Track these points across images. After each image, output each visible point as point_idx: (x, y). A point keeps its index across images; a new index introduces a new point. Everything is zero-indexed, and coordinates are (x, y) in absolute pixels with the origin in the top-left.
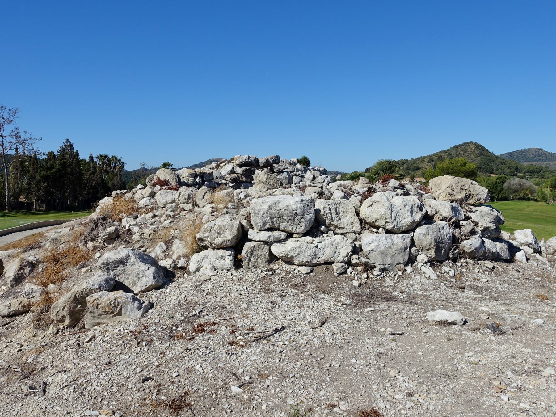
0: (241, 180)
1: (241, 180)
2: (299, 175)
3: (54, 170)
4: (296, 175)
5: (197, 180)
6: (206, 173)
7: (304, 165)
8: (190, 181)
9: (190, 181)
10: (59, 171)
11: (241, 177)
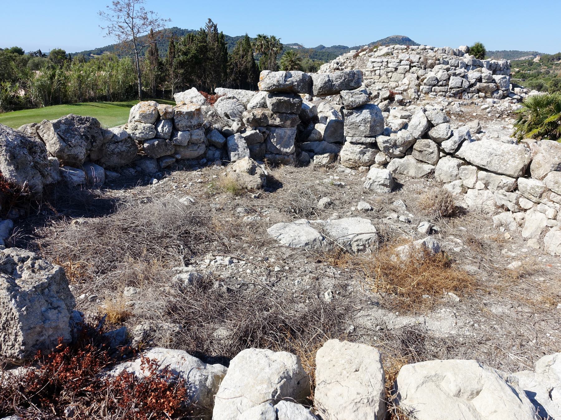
1: (270, 122)
2: (459, 74)
3: (190, 56)
4: (455, 75)
8: (137, 132)
9: (137, 132)
10: (195, 56)
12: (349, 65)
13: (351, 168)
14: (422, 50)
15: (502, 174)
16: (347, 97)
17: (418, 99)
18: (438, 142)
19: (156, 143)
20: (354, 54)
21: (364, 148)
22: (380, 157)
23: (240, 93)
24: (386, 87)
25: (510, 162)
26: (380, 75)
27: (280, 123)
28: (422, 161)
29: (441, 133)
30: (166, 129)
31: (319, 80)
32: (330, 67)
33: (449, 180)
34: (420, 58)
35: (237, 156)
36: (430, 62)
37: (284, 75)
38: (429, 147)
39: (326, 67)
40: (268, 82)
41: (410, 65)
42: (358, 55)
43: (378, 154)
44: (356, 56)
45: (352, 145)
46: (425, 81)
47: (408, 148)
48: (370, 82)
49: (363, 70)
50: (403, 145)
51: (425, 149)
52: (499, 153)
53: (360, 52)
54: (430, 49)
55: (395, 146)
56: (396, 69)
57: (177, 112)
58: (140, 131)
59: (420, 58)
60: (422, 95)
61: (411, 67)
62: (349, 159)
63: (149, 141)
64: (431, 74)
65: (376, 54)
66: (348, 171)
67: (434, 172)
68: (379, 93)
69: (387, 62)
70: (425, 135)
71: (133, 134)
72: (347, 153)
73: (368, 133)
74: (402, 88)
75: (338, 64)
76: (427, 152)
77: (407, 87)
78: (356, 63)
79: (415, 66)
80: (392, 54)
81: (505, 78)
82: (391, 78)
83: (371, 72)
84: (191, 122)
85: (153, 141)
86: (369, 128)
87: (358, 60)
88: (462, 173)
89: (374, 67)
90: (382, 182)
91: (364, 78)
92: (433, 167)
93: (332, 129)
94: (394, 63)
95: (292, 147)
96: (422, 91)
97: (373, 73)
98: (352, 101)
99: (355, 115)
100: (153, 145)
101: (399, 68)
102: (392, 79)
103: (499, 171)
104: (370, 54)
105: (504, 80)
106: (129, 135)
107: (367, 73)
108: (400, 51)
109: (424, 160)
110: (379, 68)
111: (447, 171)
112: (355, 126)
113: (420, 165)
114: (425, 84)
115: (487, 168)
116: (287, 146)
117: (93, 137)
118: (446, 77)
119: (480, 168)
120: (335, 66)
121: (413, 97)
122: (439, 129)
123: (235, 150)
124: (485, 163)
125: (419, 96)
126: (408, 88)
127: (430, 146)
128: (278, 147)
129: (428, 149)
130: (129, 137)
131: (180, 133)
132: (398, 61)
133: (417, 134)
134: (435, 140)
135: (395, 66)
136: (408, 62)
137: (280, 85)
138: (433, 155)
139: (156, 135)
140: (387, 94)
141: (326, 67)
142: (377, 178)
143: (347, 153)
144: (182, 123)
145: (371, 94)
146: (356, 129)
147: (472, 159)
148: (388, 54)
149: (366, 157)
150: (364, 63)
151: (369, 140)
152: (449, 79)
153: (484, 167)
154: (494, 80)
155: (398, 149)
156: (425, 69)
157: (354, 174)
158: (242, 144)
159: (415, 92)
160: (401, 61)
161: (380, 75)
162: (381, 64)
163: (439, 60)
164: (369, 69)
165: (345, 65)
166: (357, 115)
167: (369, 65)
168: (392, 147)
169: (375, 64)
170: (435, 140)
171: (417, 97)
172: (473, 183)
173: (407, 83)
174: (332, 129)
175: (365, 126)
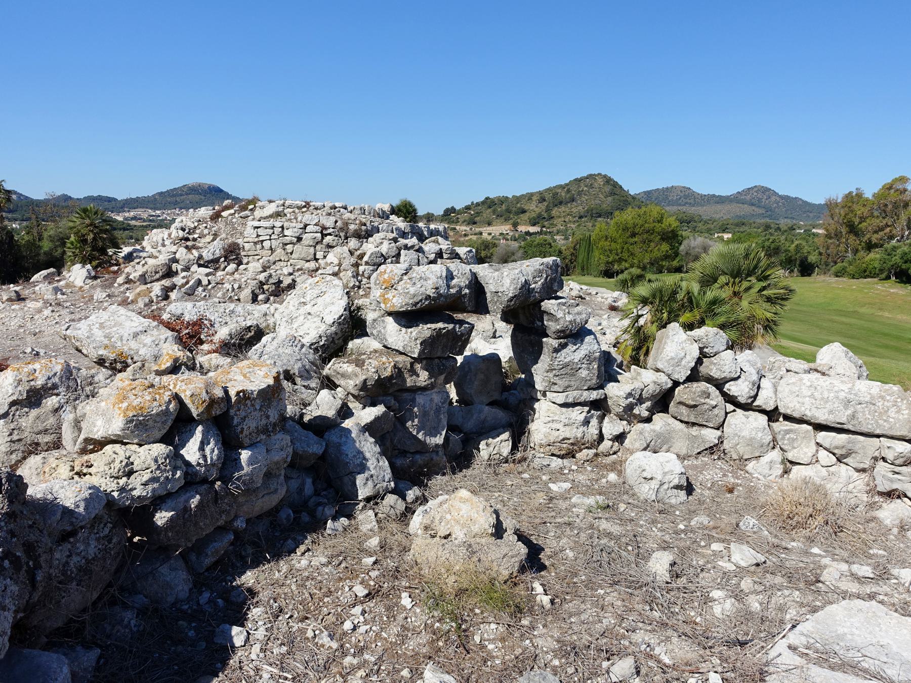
0: (410, 381)
1: (410, 381)
2: (413, 247)
4: (406, 247)
5: (191, 452)
6: (244, 396)
7: (406, 217)
11: (413, 372)
12: (206, 232)
13: (562, 457)
14: (331, 208)
15: (878, 436)
16: (560, 315)
17: (359, 287)
18: (719, 384)
19: (195, 501)
20: (211, 213)
21: (589, 412)
22: (612, 427)
23: (232, 312)
24: (299, 270)
25: (892, 413)
26: (271, 249)
27: (428, 382)
28: (694, 424)
29: (727, 369)
30: (213, 451)
31: (507, 282)
32: (170, 235)
33: (757, 455)
34: (336, 222)
35: (370, 483)
36: (352, 227)
37: (444, 274)
38: (708, 396)
39: (161, 235)
40: (412, 290)
41: (321, 233)
42: (221, 216)
43: (606, 419)
44: (216, 217)
45: (564, 410)
46: (366, 258)
47: (662, 401)
48: (269, 261)
49: (240, 241)
50: (652, 397)
51: (703, 401)
52: (867, 399)
53: (223, 211)
54: (342, 207)
55: (641, 401)
56: (299, 239)
57: (238, 393)
58: (147, 476)
59: (336, 222)
60: (365, 280)
61: (324, 236)
62: (564, 439)
63: (170, 503)
64: (369, 247)
65: (258, 213)
66: (556, 463)
67: (722, 442)
68: (294, 281)
69: (282, 227)
70: (694, 376)
71: (122, 490)
72: (555, 426)
73: (594, 381)
75: (183, 229)
76: (706, 407)
77: (337, 268)
78: (220, 229)
79: (330, 234)
80: (285, 215)
81: (470, 251)
82: (291, 253)
83: (255, 243)
84: (268, 417)
85: (182, 499)
86: (596, 372)
87: (221, 224)
88: (783, 439)
89: (258, 236)
90: (676, 482)
91: (242, 254)
92: (719, 433)
93: (482, 376)
94: (296, 230)
95: (444, 433)
96: (363, 275)
97: (259, 246)
98: (570, 322)
99: (571, 348)
100: (187, 509)
101: (304, 236)
102: (294, 256)
103: (878, 432)
105: (471, 255)
106: (108, 495)
107: (247, 246)
108: (297, 211)
109: (700, 421)
110: (268, 237)
111: (751, 439)
112: (571, 369)
113: (694, 431)
114: (367, 263)
115: (845, 427)
116: (434, 433)
117: (29, 548)
118: (394, 252)
119: (820, 427)
120: (181, 234)
121: (351, 285)
122: (722, 362)
123: (363, 468)
124: (844, 420)
125: (360, 282)
127: (709, 394)
128: (420, 436)
129: (707, 400)
130: (110, 503)
131: (245, 455)
132: (302, 226)
133: (681, 376)
134: (710, 380)
135: (297, 235)
136: (318, 228)
137: (440, 295)
138: (716, 411)
139: (186, 474)
141: (161, 235)
142: (665, 474)
143: (555, 426)
144: (251, 425)
145: (280, 282)
146: (573, 375)
147: (808, 413)
148: (278, 215)
149: (593, 430)
150: (234, 229)
151: (594, 395)
152: (398, 255)
153: (839, 426)
154: (457, 254)
155: (644, 406)
156: (346, 238)
157: (574, 467)
158: (369, 447)
159: (353, 277)
160: (306, 226)
161: (271, 249)
162: (271, 231)
163: (365, 225)
164: (251, 240)
165: (198, 231)
166: (575, 347)
167: (250, 233)
168: (636, 405)
170: (710, 380)
171: (357, 284)
172: (810, 454)
173: (336, 262)
174: (482, 376)
175: (588, 369)
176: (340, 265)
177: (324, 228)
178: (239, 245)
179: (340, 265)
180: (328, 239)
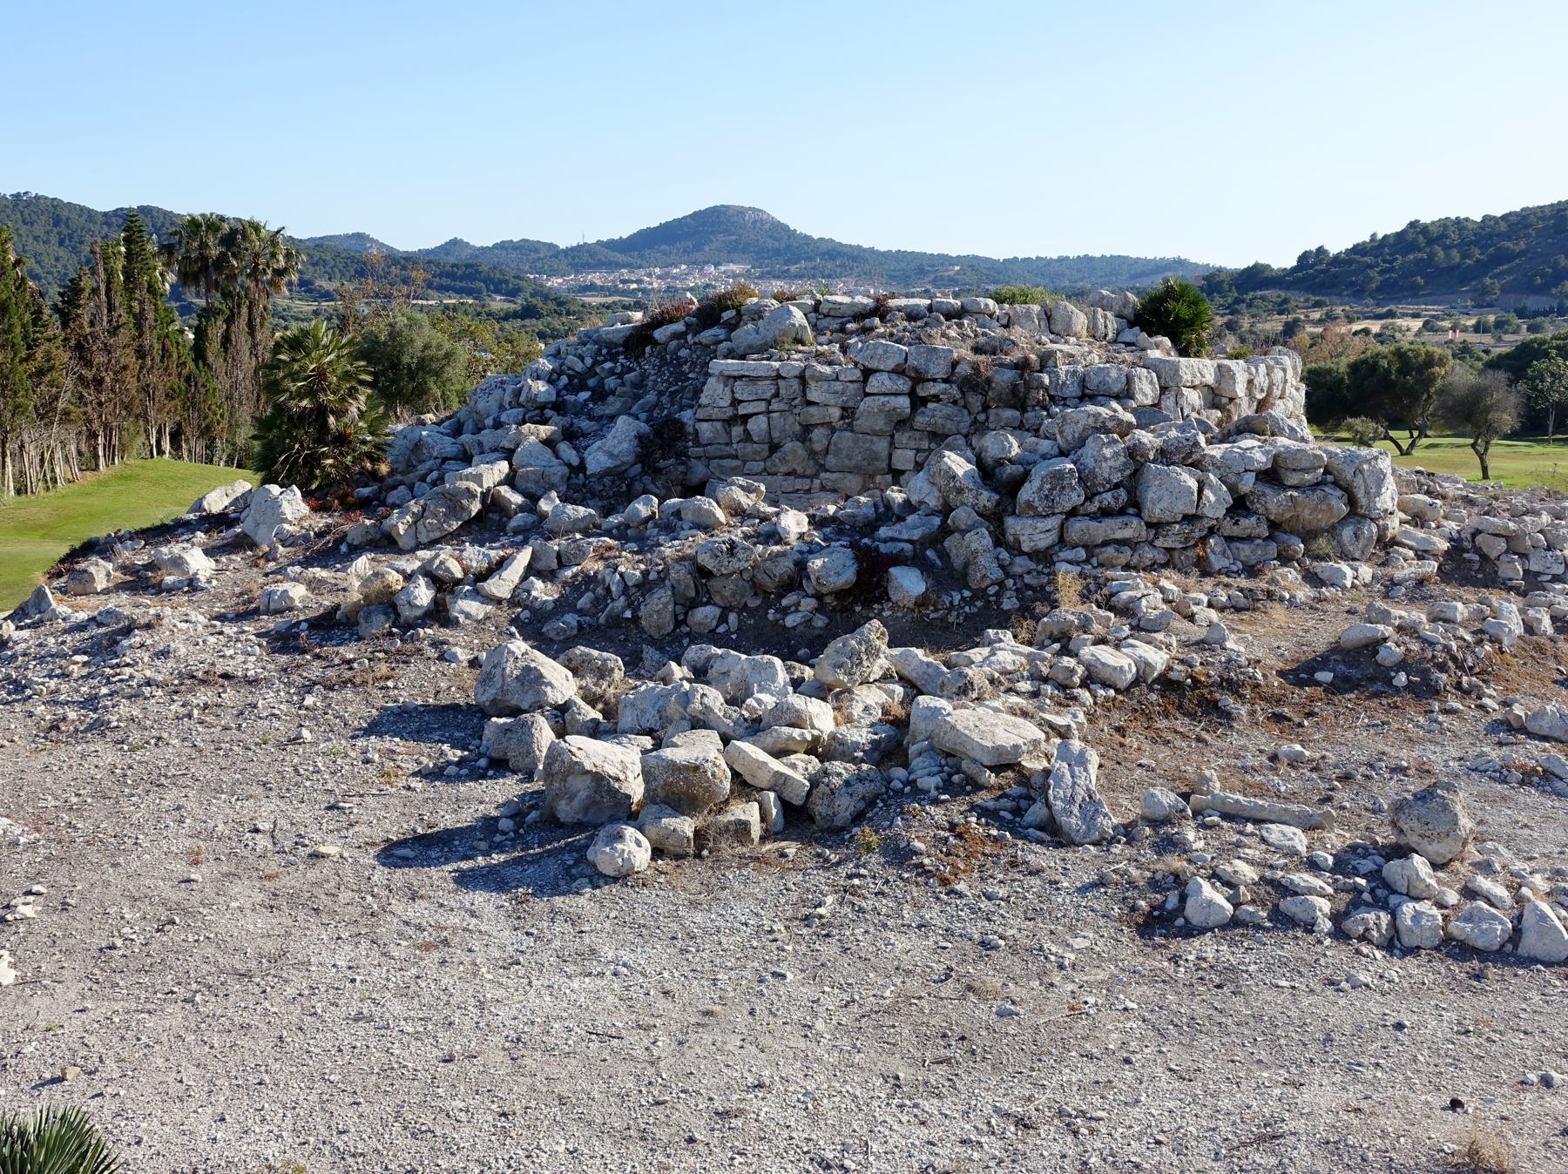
41: (912, 394)
42: (655, 343)
49: (686, 416)
74: (913, 528)
77: (937, 521)
78: (644, 376)
83: (729, 422)
89: (735, 402)
91: (694, 451)
97: (737, 431)
102: (831, 461)
104: (706, 336)
110: (762, 407)
126: (946, 531)
136: (903, 385)
140: (848, 576)
160: (867, 373)
164: (716, 414)
169: (742, 391)
173: (933, 502)
176: (946, 510)
177: (919, 378)
178: (683, 425)
179: (946, 510)
180: (935, 414)
